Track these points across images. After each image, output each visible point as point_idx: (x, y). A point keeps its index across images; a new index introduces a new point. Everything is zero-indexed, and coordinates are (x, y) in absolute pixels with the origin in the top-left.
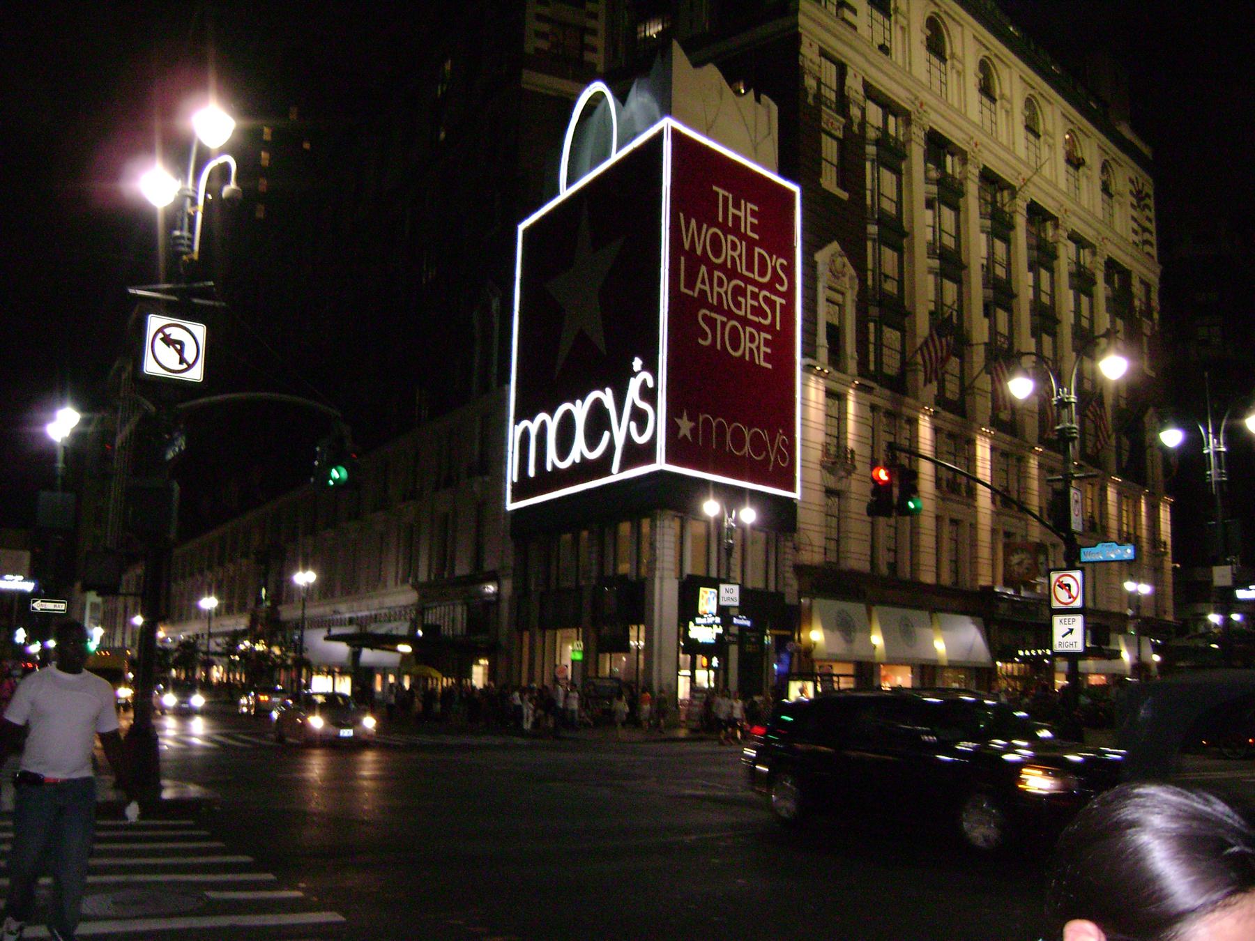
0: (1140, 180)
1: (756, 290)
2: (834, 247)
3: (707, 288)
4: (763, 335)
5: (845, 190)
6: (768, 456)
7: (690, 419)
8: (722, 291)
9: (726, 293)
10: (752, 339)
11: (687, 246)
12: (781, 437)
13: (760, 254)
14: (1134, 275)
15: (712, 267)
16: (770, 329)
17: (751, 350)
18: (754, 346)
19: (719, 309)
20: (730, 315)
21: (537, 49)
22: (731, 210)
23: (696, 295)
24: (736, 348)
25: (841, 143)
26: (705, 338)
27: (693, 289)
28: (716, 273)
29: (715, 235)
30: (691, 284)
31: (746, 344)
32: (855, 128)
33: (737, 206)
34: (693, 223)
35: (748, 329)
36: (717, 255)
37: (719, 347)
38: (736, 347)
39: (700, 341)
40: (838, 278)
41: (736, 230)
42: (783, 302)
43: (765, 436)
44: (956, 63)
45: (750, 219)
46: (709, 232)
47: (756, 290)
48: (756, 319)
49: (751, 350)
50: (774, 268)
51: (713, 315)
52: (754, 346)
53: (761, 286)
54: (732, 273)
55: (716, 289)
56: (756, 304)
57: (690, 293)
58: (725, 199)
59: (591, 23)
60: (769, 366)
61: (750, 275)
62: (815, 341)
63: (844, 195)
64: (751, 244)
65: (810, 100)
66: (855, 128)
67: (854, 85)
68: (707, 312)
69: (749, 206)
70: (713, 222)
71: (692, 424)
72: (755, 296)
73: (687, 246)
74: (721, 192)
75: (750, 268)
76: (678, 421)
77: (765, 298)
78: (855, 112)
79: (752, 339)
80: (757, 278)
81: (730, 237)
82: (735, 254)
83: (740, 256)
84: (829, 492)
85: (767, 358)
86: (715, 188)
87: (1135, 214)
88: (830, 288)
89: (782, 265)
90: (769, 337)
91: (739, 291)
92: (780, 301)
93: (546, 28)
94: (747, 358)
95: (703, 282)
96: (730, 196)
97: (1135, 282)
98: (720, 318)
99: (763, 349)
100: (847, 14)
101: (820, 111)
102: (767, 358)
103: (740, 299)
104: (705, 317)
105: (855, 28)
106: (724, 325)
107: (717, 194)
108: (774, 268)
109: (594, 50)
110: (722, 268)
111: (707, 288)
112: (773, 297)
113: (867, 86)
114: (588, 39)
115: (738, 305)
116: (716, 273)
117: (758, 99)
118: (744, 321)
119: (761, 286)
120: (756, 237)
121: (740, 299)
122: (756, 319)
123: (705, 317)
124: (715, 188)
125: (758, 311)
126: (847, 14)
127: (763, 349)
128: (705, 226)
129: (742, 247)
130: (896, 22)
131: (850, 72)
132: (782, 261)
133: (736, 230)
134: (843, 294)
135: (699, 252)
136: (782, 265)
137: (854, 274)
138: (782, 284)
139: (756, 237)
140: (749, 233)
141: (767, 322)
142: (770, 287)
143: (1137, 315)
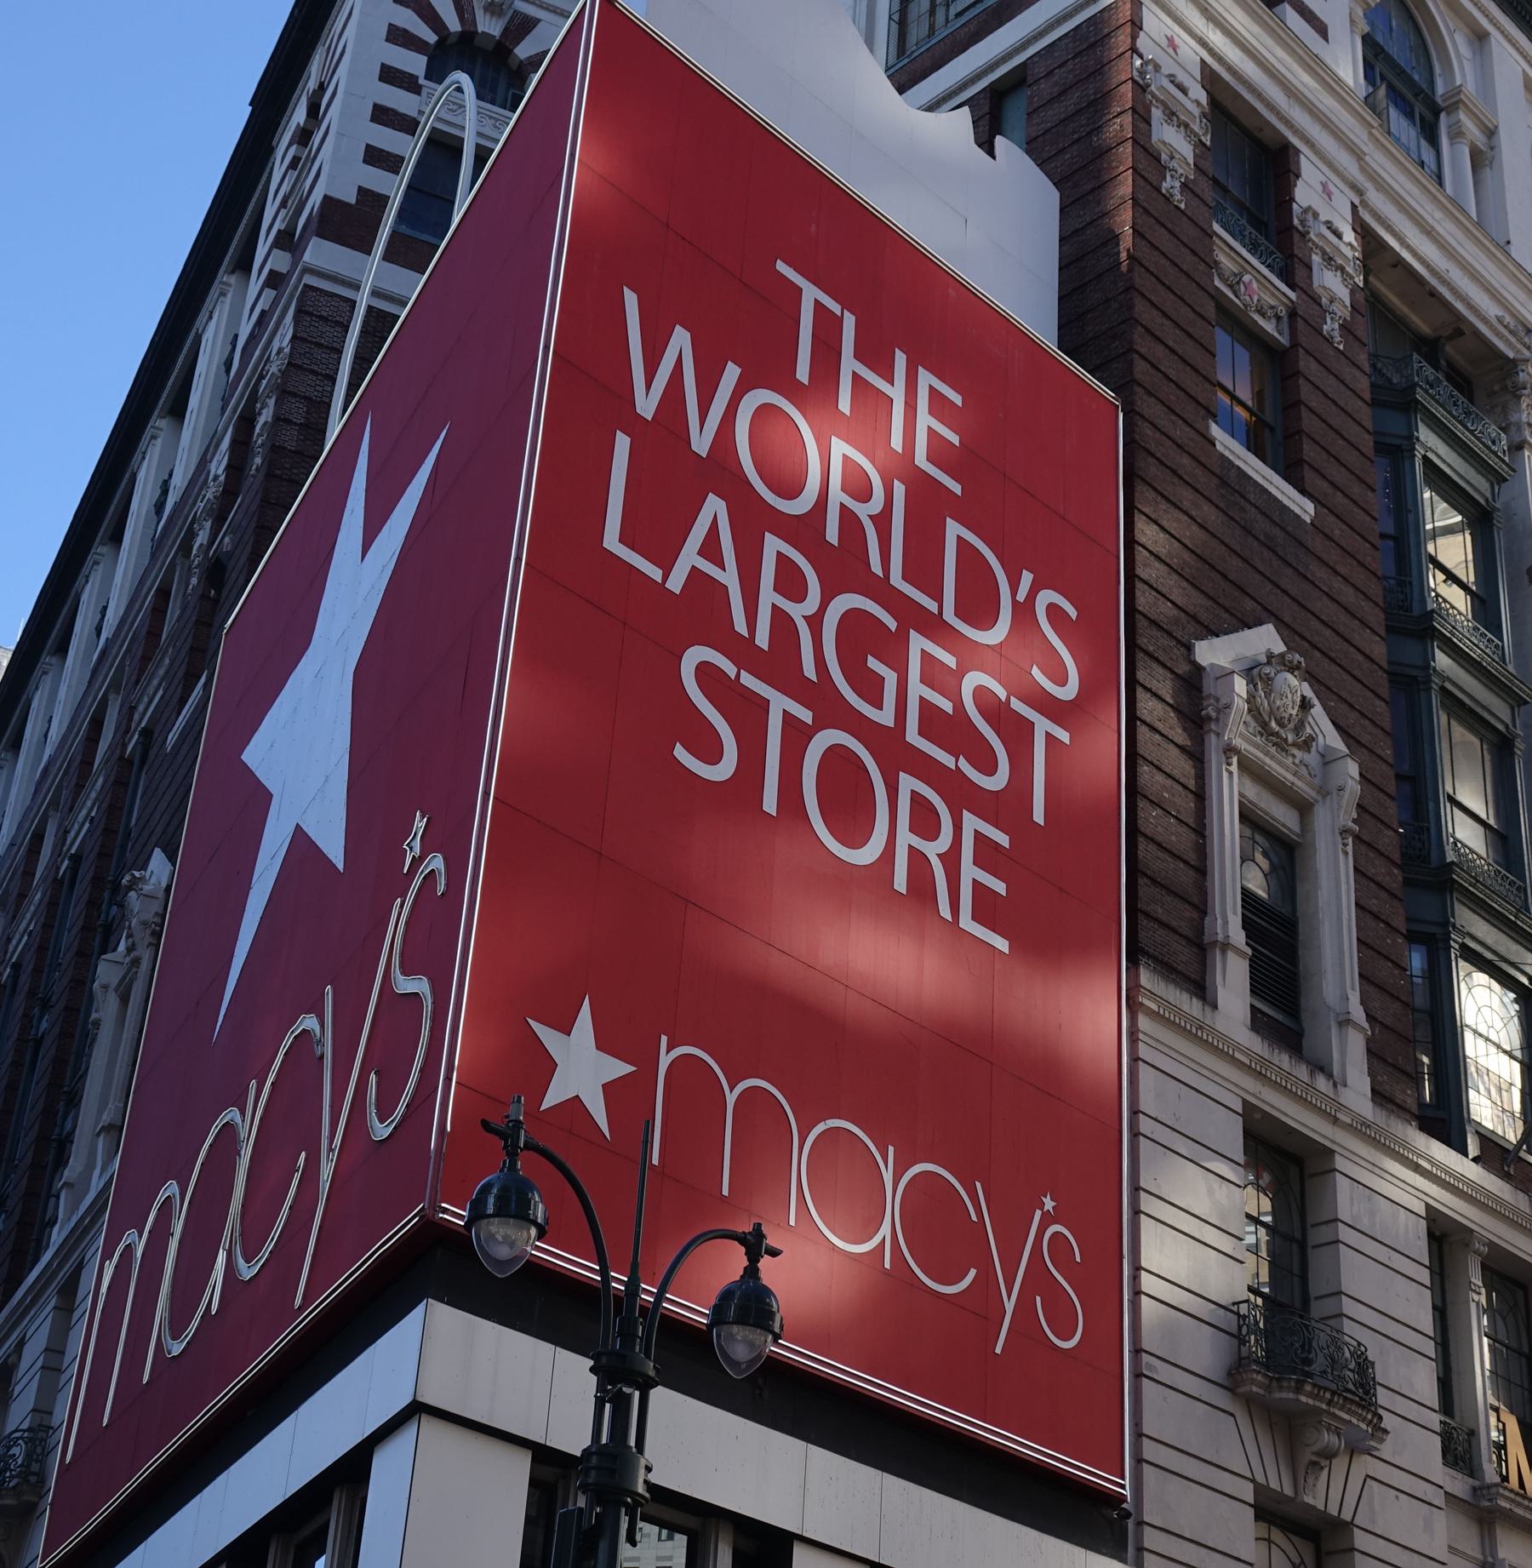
1: (950, 661)
3: (729, 577)
4: (971, 822)
8: (798, 612)
9: (815, 622)
10: (924, 821)
11: (646, 405)
12: (1045, 1227)
16: (1006, 807)
21: (362, 191)
22: (849, 364)
23: (676, 583)
26: (712, 755)
28: (773, 545)
32: (1330, 327)
34: (681, 339)
35: (908, 783)
40: (1282, 745)
43: (977, 1206)
47: (950, 661)
48: (946, 759)
49: (915, 855)
51: (747, 680)
52: (933, 850)
54: (844, 565)
55: (768, 596)
56: (947, 706)
57: (655, 573)
58: (827, 326)
61: (931, 605)
62: (1200, 931)
63: (1304, 508)
69: (925, 379)
71: (622, 1069)
73: (646, 405)
74: (811, 294)
76: (547, 1036)
83: (882, 521)
89: (1052, 609)
92: (1043, 726)
96: (849, 321)
98: (780, 704)
99: (970, 872)
102: (987, 908)
106: (796, 736)
111: (729, 577)
115: (871, 689)
116: (773, 545)
118: (892, 750)
120: (957, 488)
122: (946, 759)
123: (705, 672)
127: (970, 872)
128: (732, 373)
132: (1046, 597)
134: (1304, 808)
135: (701, 443)
139: (957, 488)
141: (996, 782)
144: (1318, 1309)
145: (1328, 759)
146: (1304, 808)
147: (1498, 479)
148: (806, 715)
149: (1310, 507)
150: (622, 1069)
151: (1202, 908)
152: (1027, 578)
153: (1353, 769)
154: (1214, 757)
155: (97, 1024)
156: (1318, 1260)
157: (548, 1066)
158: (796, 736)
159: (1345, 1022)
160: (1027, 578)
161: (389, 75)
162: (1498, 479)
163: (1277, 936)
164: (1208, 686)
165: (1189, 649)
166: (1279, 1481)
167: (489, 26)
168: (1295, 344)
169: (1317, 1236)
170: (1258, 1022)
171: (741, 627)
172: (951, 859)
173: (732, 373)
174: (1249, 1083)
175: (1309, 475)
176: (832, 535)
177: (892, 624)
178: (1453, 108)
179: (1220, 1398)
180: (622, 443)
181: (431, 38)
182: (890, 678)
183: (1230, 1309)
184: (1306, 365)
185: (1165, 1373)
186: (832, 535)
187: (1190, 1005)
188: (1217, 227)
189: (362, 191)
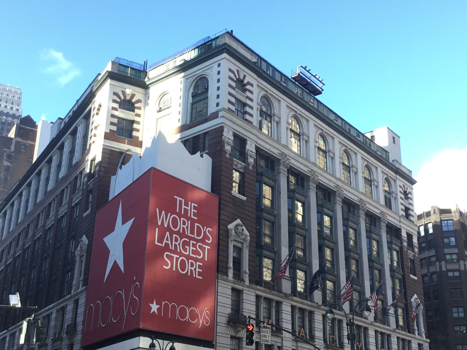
0: (406, 186)
1: (195, 243)
2: (238, 221)
3: (169, 242)
4: (198, 263)
5: (244, 196)
6: (198, 320)
7: (157, 304)
8: (177, 243)
9: (179, 244)
10: (192, 265)
11: (159, 223)
13: (197, 226)
14: (403, 231)
15: (172, 233)
17: (191, 270)
18: (193, 269)
19: (175, 252)
20: (181, 254)
21: (110, 130)
22: (183, 207)
23: (163, 246)
24: (183, 269)
25: (242, 175)
26: (167, 266)
27: (162, 244)
28: (174, 235)
29: (174, 218)
30: (160, 241)
31: (188, 268)
32: (251, 168)
33: (186, 204)
34: (163, 212)
35: (190, 261)
36: (175, 227)
37: (174, 269)
38: (183, 268)
39: (164, 267)
40: (239, 236)
41: (185, 216)
42: (209, 248)
44: (305, 136)
45: (193, 210)
46: (171, 217)
47: (195, 243)
48: (194, 256)
49: (191, 270)
50: (205, 233)
51: (172, 255)
53: (198, 241)
54: (182, 235)
55: (174, 242)
57: (160, 245)
58: (181, 202)
59: (137, 119)
60: (201, 278)
61: (193, 236)
63: (244, 198)
64: (193, 222)
65: (228, 156)
66: (251, 168)
67: (250, 147)
68: (169, 254)
69: (193, 204)
70: (173, 212)
71: (159, 306)
72: (194, 245)
73: (159, 223)
74: (179, 199)
75: (192, 233)
76: (150, 305)
77: (199, 246)
78: (251, 160)
79: (192, 265)
80: (196, 237)
81: (182, 219)
82: (185, 227)
83: (187, 227)
84: (232, 337)
85: (200, 274)
86: (175, 197)
87: (403, 202)
88: (235, 240)
89: (209, 231)
90: (201, 264)
91: (185, 243)
92: (207, 247)
93: (115, 121)
94: (189, 274)
95: (167, 240)
96: (183, 200)
97: (404, 234)
98: (175, 256)
100: (248, 117)
101: (232, 160)
102: (200, 274)
103: (186, 247)
104: (167, 256)
105: (252, 123)
106: (177, 259)
107: (177, 199)
108: (205, 233)
109: (138, 130)
110: (178, 233)
112: (204, 246)
113: (257, 149)
114: (135, 126)
116: (174, 235)
117: (202, 156)
118: (188, 257)
119: (198, 241)
120: (196, 218)
121: (186, 247)
122: (194, 256)
123: (167, 255)
124: (175, 197)
125: (194, 252)
126: (248, 117)
127: (197, 270)
128: (169, 214)
129: (189, 223)
130: (274, 120)
131: (249, 142)
133: (185, 216)
134: (242, 243)
135: (166, 226)
136: (209, 231)
137: (249, 234)
138: (209, 240)
139: (196, 218)
140: (192, 217)
142: (203, 241)
143: (405, 250)
144: (241, 310)
145: (246, 236)
146: (242, 243)
147: (275, 181)
148: (178, 256)
149: (245, 198)
150: (159, 306)
151: (227, 262)
152: (205, 227)
153: (249, 238)
154: (230, 242)
155: (76, 260)
156: (241, 304)
157: (151, 308)
158: (177, 259)
159: (246, 273)
160: (205, 227)
161: (113, 109)
162: (275, 181)
163: (238, 262)
164: (230, 232)
165: (227, 226)
166: (233, 334)
167: (128, 98)
168: (245, 172)
169: (241, 301)
170: (234, 277)
171: (171, 248)
172: (195, 269)
173: (169, 214)
174: (232, 284)
175: (246, 193)
176: (181, 232)
177: (188, 240)
178: (274, 115)
179: (226, 326)
180: (157, 229)
181: (119, 100)
182: (188, 248)
183: (229, 314)
184: (247, 175)
185: (220, 324)
186: (181, 232)
187: (225, 277)
188: (234, 159)
189: (110, 130)
